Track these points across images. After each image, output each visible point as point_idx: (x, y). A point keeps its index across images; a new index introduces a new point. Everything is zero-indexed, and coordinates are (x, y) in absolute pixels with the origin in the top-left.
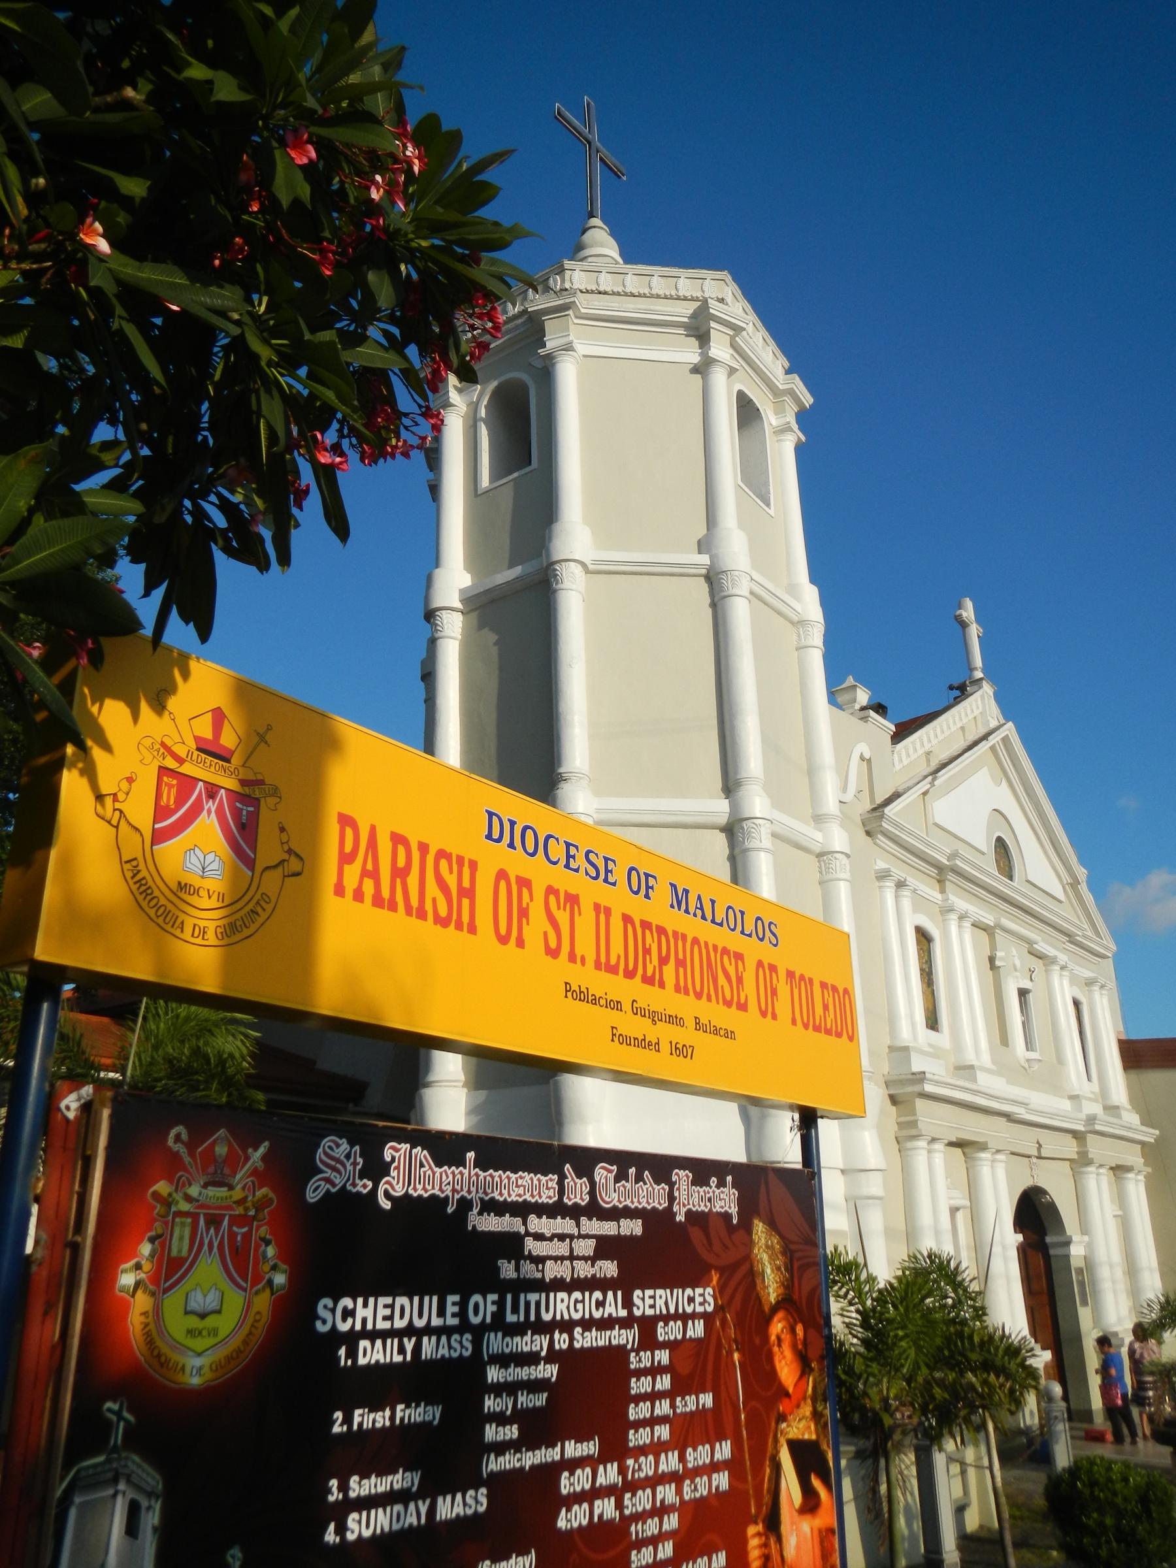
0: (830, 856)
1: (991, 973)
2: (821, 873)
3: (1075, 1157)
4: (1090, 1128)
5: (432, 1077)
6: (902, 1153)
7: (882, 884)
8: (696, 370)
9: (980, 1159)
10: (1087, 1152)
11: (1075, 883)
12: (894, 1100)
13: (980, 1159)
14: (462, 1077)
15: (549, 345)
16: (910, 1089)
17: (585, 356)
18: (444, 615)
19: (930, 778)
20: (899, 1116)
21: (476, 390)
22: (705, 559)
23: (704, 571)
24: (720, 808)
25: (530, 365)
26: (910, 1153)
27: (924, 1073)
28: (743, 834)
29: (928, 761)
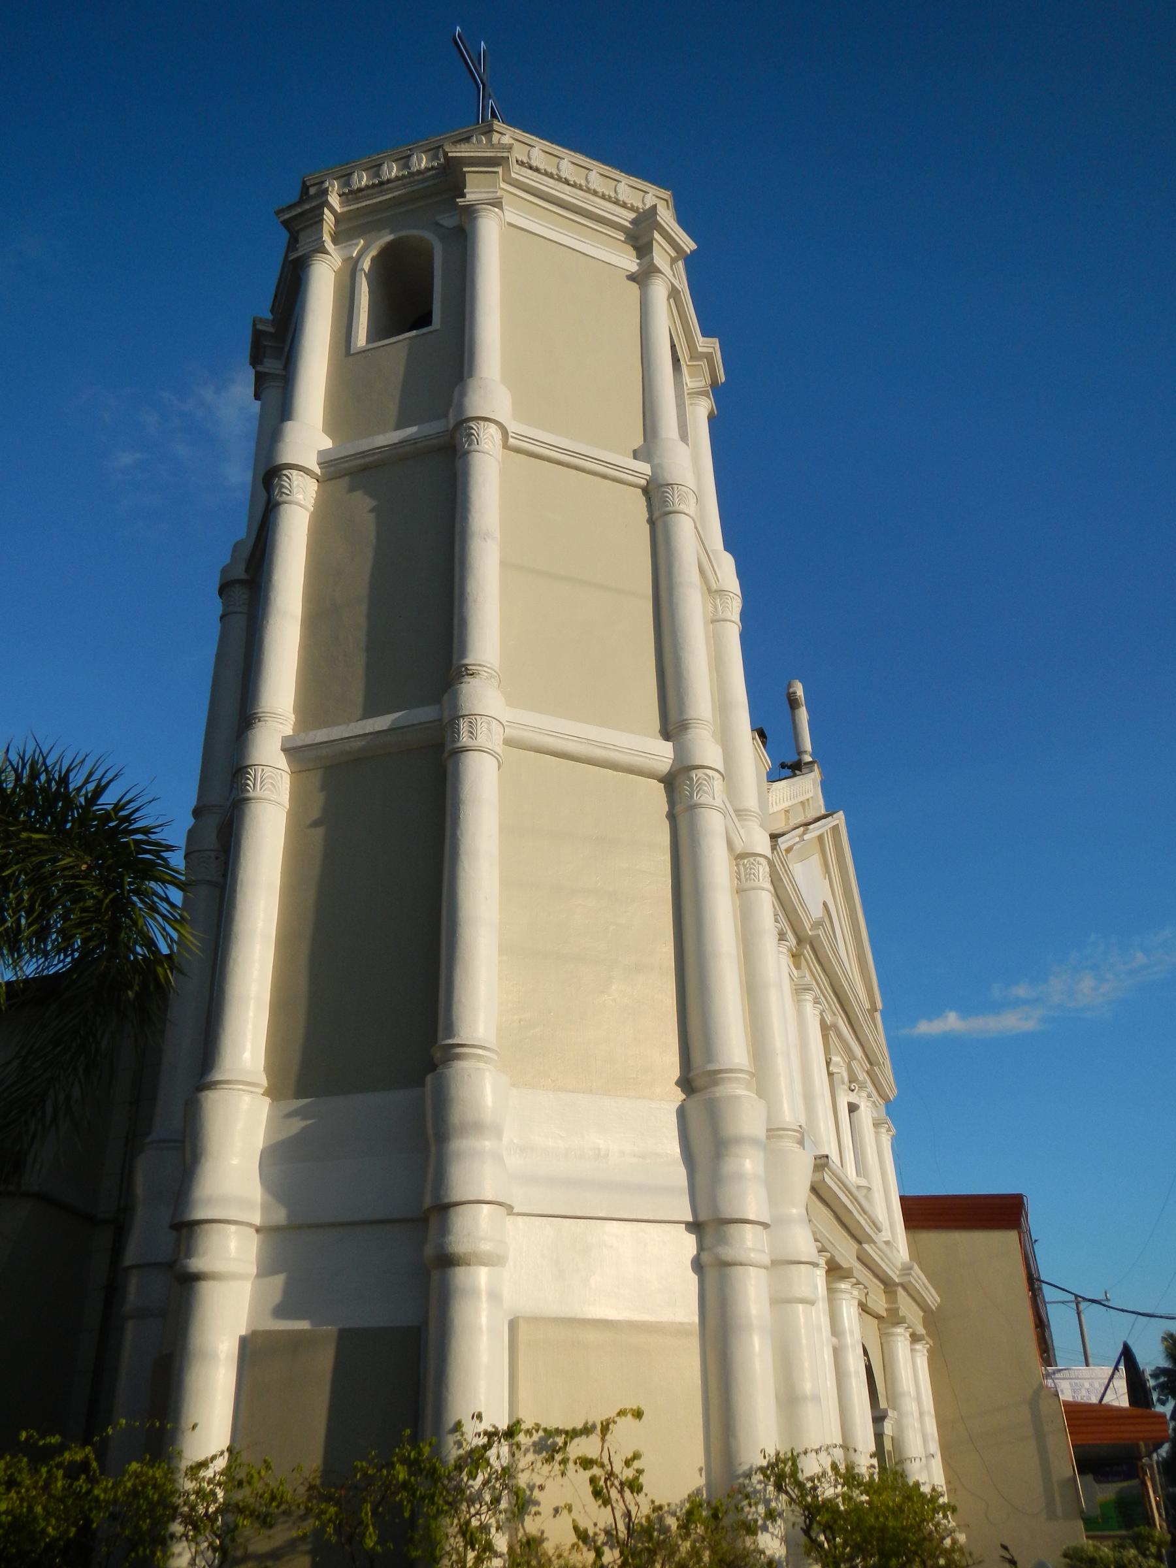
0: (752, 859)
2: (739, 879)
3: (884, 1314)
5: (217, 1076)
8: (632, 278)
9: (842, 1291)
10: (897, 1309)
11: (874, 1009)
14: (264, 1082)
15: (469, 197)
17: (510, 224)
18: (296, 477)
19: (802, 829)
21: (357, 244)
22: (645, 468)
23: (643, 482)
24: (662, 754)
25: (437, 224)
28: (691, 786)
29: (787, 819)
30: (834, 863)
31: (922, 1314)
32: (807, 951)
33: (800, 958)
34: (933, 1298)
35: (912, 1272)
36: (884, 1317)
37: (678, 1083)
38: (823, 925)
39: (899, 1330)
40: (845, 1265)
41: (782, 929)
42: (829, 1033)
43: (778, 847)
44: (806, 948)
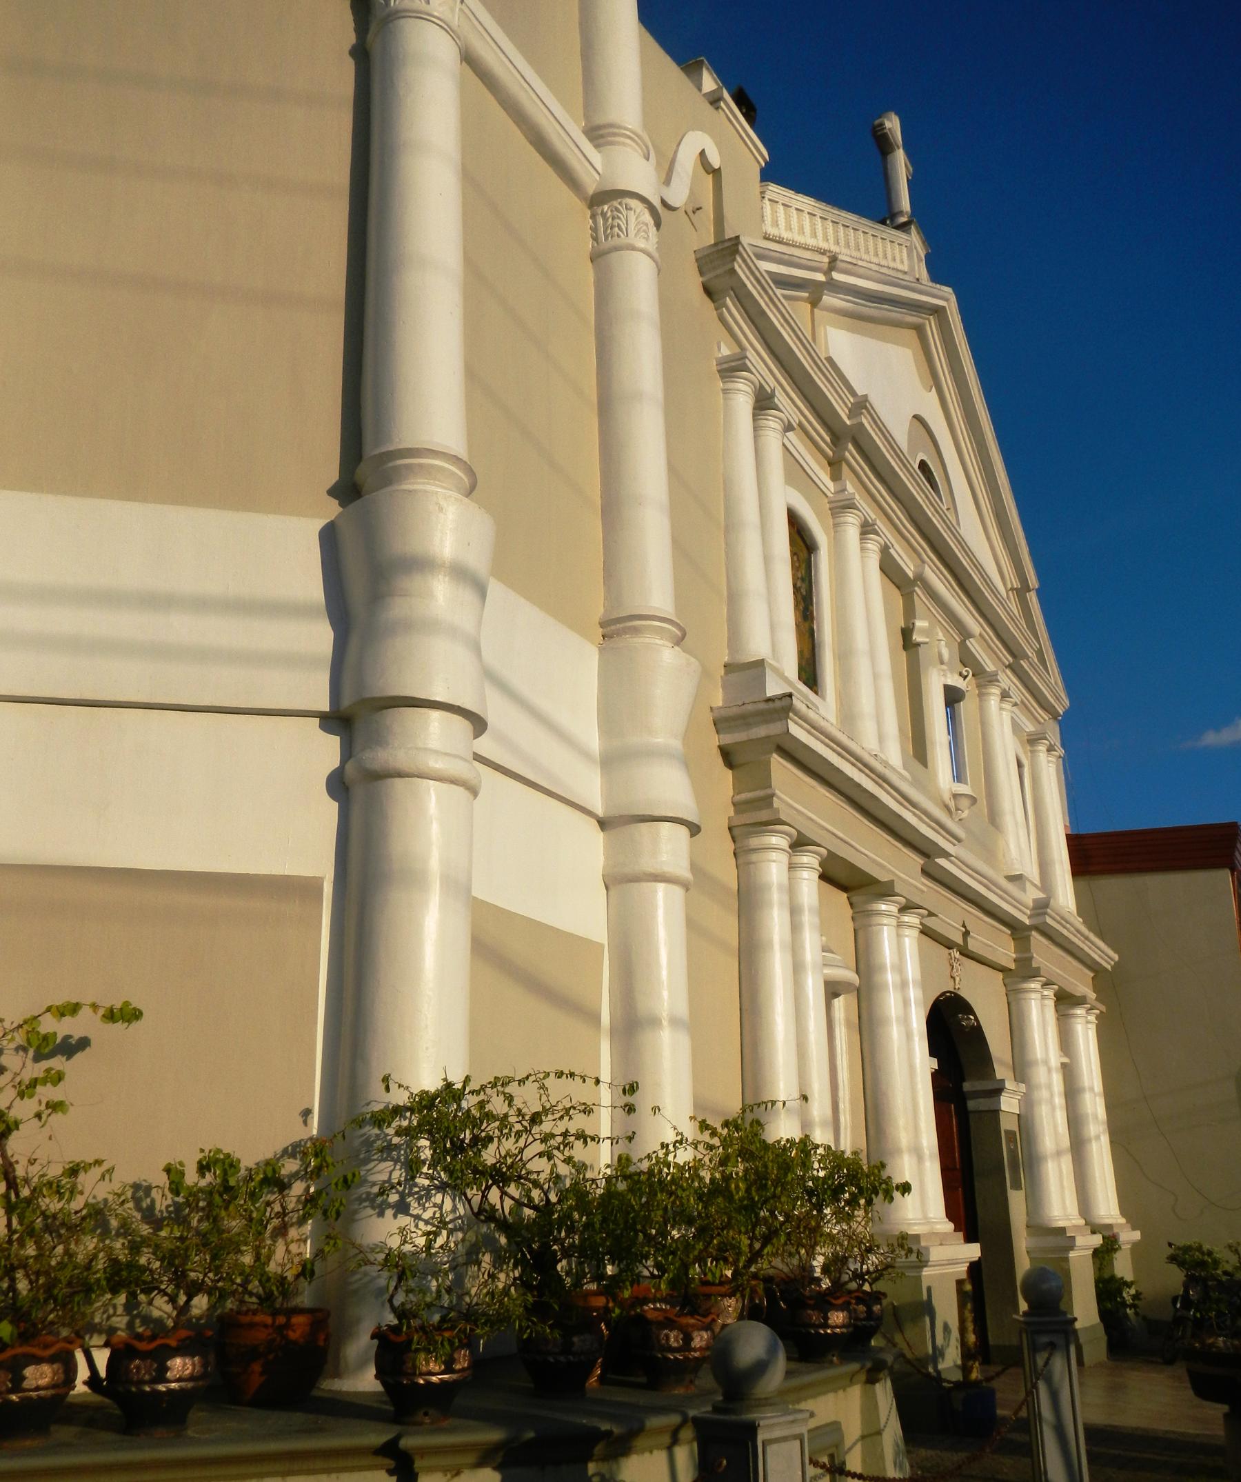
1: (904, 654)
3: (1012, 966)
4: (1037, 921)
6: (740, 861)
7: (730, 385)
9: (880, 914)
10: (1031, 958)
12: (728, 756)
13: (880, 914)
16: (761, 731)
20: (737, 789)
26: (754, 857)
27: (790, 695)
30: (947, 372)
31: (1092, 975)
32: (851, 453)
33: (841, 466)
34: (1104, 955)
35: (1048, 910)
36: (1011, 970)
37: (332, 492)
38: (866, 408)
39: (1034, 985)
40: (883, 877)
41: (761, 386)
42: (915, 591)
43: (741, 248)
44: (847, 449)
